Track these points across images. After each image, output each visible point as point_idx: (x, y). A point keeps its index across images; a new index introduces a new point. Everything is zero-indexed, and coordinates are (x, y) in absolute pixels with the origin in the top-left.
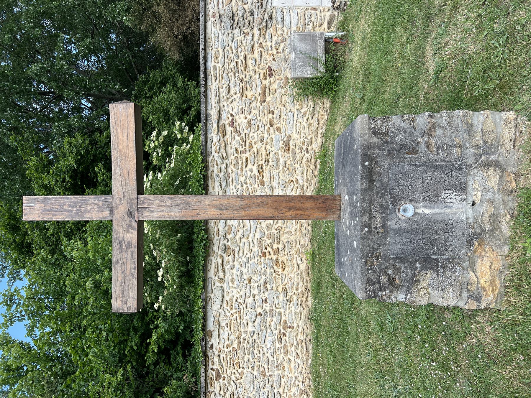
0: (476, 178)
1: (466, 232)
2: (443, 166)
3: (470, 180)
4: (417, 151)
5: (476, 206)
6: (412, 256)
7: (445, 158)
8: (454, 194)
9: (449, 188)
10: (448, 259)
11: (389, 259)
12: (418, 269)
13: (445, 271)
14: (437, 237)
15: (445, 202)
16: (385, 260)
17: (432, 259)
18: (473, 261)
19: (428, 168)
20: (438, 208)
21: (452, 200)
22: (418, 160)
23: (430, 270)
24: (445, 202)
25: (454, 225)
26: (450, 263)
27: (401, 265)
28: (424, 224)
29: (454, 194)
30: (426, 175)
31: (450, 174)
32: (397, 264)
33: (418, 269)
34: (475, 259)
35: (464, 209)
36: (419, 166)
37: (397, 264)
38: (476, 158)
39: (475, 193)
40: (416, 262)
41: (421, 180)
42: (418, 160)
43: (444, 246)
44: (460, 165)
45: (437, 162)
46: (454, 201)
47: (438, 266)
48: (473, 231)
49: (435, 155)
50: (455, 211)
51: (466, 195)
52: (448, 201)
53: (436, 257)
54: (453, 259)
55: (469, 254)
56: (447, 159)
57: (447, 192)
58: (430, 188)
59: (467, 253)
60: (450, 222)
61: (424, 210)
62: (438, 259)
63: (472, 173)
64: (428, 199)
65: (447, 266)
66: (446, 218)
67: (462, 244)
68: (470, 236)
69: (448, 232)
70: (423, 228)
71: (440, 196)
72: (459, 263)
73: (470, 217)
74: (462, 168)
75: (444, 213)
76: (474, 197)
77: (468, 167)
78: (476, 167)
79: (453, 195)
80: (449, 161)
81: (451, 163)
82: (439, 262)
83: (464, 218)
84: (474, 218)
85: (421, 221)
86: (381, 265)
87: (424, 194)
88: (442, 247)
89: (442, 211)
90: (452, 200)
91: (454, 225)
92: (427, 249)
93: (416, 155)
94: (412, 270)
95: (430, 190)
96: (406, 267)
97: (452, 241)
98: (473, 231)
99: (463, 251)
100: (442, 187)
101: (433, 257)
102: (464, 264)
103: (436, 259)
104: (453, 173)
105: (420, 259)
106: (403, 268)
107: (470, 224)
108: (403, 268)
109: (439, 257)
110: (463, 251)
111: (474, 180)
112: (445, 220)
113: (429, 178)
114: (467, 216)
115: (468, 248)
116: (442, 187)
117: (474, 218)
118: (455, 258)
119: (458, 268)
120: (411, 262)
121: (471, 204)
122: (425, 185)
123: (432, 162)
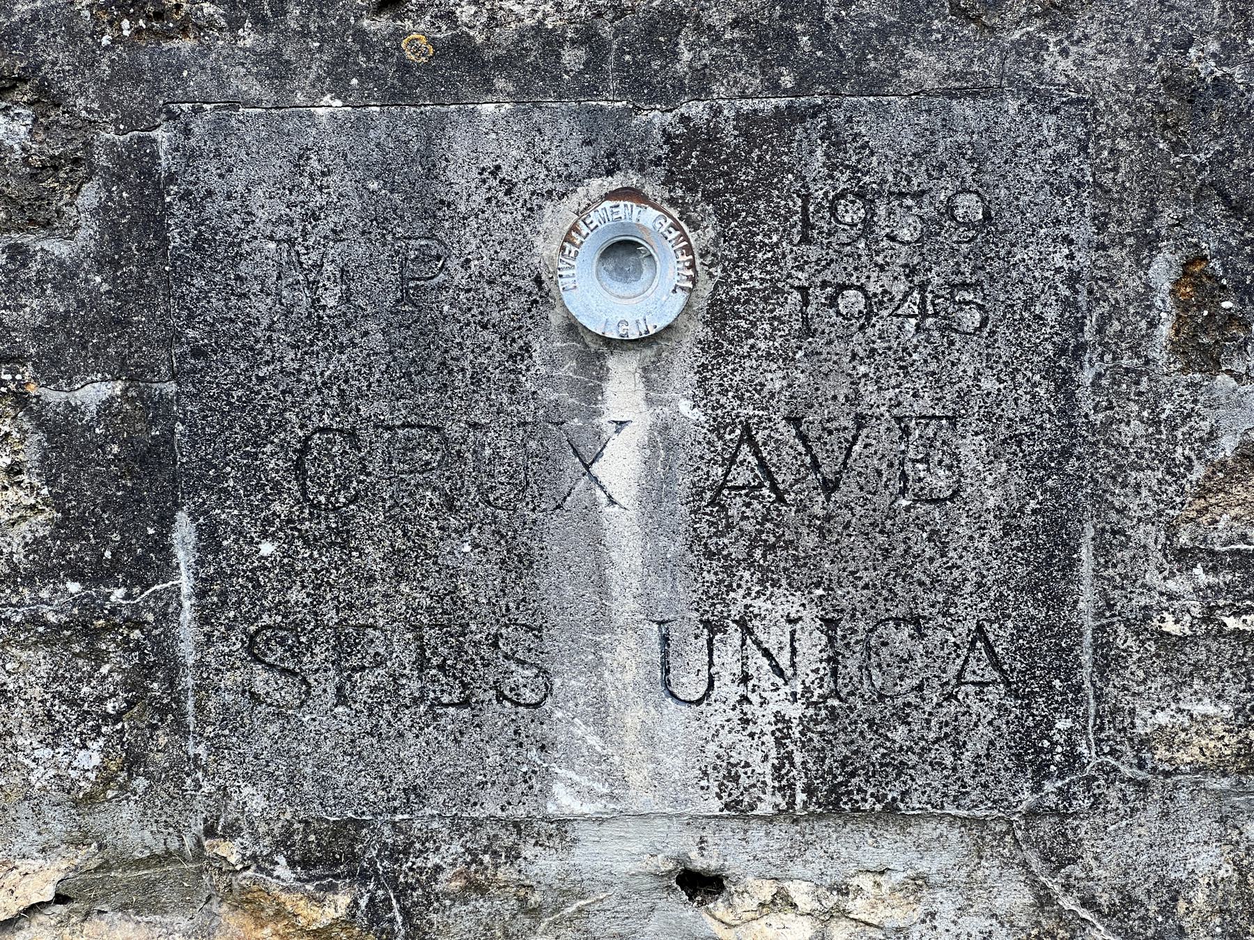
0: (946, 904)
1: (425, 817)
2: (1056, 600)
3: (923, 849)
4: (1211, 362)
5: (679, 909)
6: (178, 336)
7: (1140, 624)
8: (794, 711)
9: (851, 665)
10: (173, 669)
11: (130, 120)
12: (53, 396)
13: (52, 637)
14: (374, 559)
15: (713, 627)
16: (128, 74)
17: (166, 522)
18: (166, 894)
19: (1040, 467)
20: (659, 565)
21: (728, 689)
22: (1119, 374)
23: (57, 501)
24: (713, 627)
25: (495, 715)
26: (135, 685)
27: (88, 233)
28: (499, 440)
29: (794, 711)
30: (971, 447)
31: (980, 668)
32: (90, 195)
33: (53, 396)
34: (186, 903)
35: (643, 800)
36: (1064, 384)
37: (90, 195)
38: (1130, 901)
39: (800, 893)
40: (122, 369)
41: (924, 405)
42: (1119, 374)
43: (296, 628)
44: (1073, 758)
45: (1102, 549)
46: (719, 714)
47: (101, 575)
48: (448, 883)
49: (1172, 530)
50: (633, 717)
51: (786, 813)
52: (728, 659)
53: (184, 556)
54: (170, 711)
55: (230, 851)
56: (1124, 639)
57: (812, 645)
58: (849, 490)
59: (232, 831)
60: (522, 675)
61: (636, 433)
62: (167, 568)
63: (989, 868)
64: (742, 476)
65: (99, 658)
66: (557, 640)
67: (322, 782)
68: (395, 854)
69: (422, 664)
70: (454, 430)
71: (767, 579)
72: (134, 761)
73: (580, 857)
74: (1041, 773)
75: (602, 621)
76: (767, 891)
77: (1046, 826)
78: (1044, 900)
79: (779, 702)
80: (1108, 662)
81: (1086, 674)
82: (138, 580)
83: (564, 801)
84: (567, 894)
85: (525, 411)
86: (73, 36)
87: (787, 432)
88: (281, 607)
89: (625, 606)
90: (728, 689)
91: (495, 715)
92: (251, 472)
93: (1176, 348)
94: (38, 333)
95: (829, 487)
96: (66, 275)
97: (341, 697)
98: (448, 883)
99: (254, 799)
100: (859, 596)
101: (184, 531)
102: (128, 812)
103: (163, 548)
104: (994, 694)
105: (158, 409)
106: (59, 249)
107: (513, 855)
108: (59, 249)
109: (185, 582)
110: (254, 799)
111: (920, 883)
112: (536, 630)
113: (940, 481)
114: (584, 831)
115: (284, 842)
116: (859, 596)
117: (567, 894)
118: (180, 728)
119: (91, 758)
120: (122, 323)
121: (699, 863)
122: (880, 437)
123: (1098, 498)
